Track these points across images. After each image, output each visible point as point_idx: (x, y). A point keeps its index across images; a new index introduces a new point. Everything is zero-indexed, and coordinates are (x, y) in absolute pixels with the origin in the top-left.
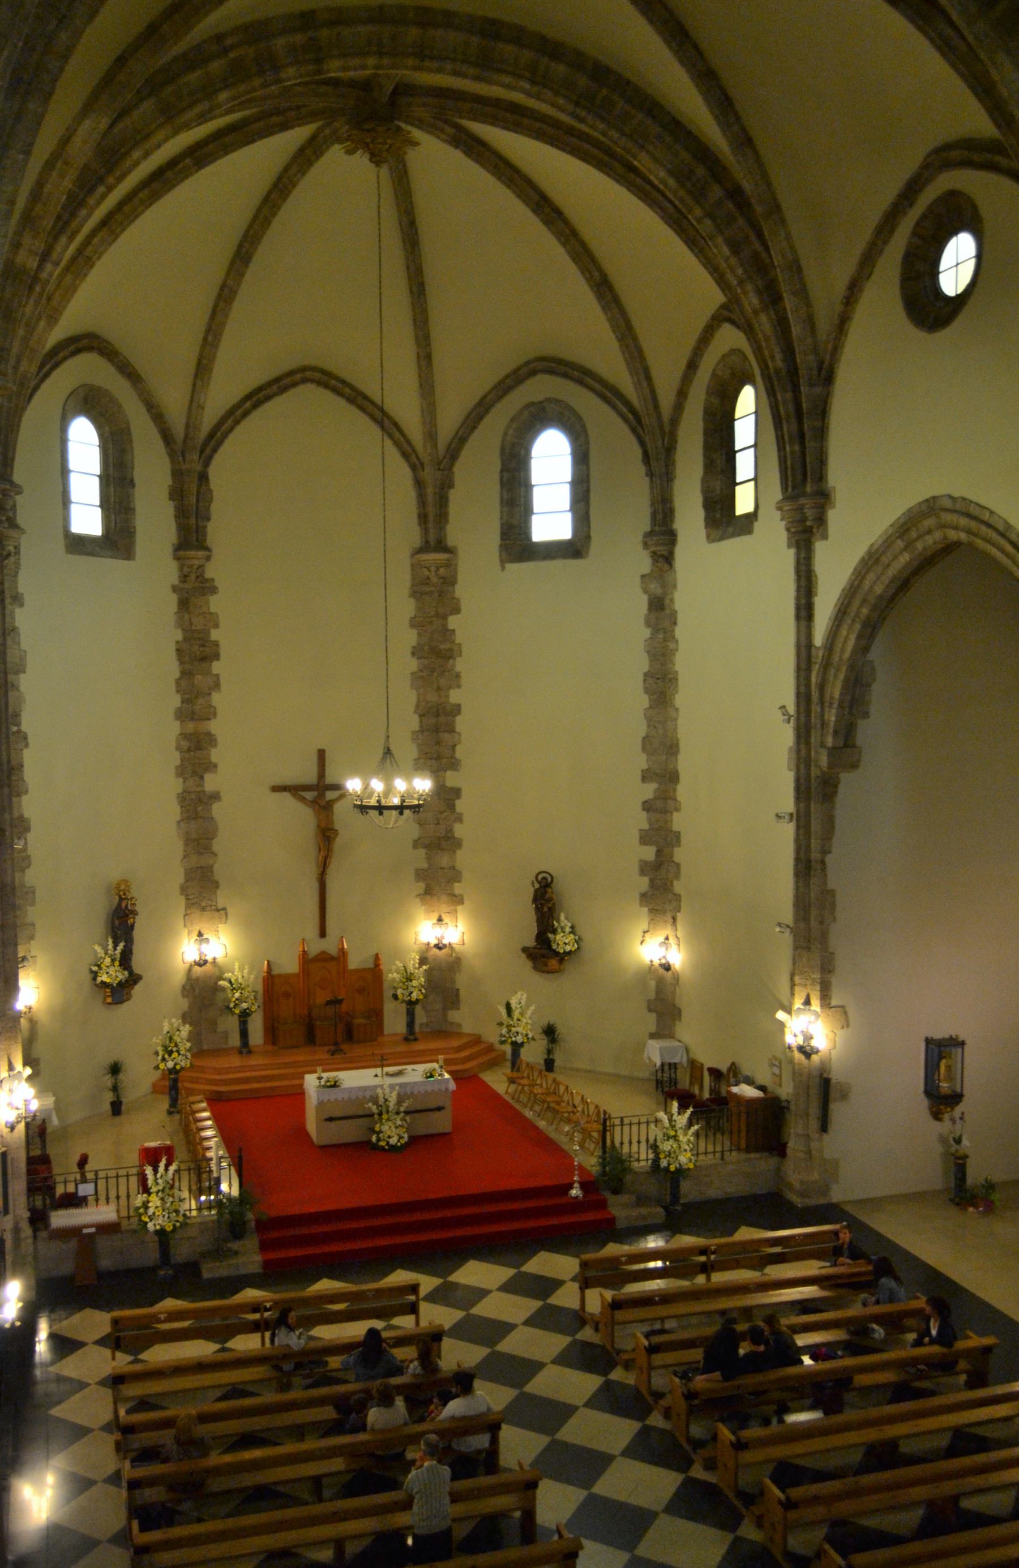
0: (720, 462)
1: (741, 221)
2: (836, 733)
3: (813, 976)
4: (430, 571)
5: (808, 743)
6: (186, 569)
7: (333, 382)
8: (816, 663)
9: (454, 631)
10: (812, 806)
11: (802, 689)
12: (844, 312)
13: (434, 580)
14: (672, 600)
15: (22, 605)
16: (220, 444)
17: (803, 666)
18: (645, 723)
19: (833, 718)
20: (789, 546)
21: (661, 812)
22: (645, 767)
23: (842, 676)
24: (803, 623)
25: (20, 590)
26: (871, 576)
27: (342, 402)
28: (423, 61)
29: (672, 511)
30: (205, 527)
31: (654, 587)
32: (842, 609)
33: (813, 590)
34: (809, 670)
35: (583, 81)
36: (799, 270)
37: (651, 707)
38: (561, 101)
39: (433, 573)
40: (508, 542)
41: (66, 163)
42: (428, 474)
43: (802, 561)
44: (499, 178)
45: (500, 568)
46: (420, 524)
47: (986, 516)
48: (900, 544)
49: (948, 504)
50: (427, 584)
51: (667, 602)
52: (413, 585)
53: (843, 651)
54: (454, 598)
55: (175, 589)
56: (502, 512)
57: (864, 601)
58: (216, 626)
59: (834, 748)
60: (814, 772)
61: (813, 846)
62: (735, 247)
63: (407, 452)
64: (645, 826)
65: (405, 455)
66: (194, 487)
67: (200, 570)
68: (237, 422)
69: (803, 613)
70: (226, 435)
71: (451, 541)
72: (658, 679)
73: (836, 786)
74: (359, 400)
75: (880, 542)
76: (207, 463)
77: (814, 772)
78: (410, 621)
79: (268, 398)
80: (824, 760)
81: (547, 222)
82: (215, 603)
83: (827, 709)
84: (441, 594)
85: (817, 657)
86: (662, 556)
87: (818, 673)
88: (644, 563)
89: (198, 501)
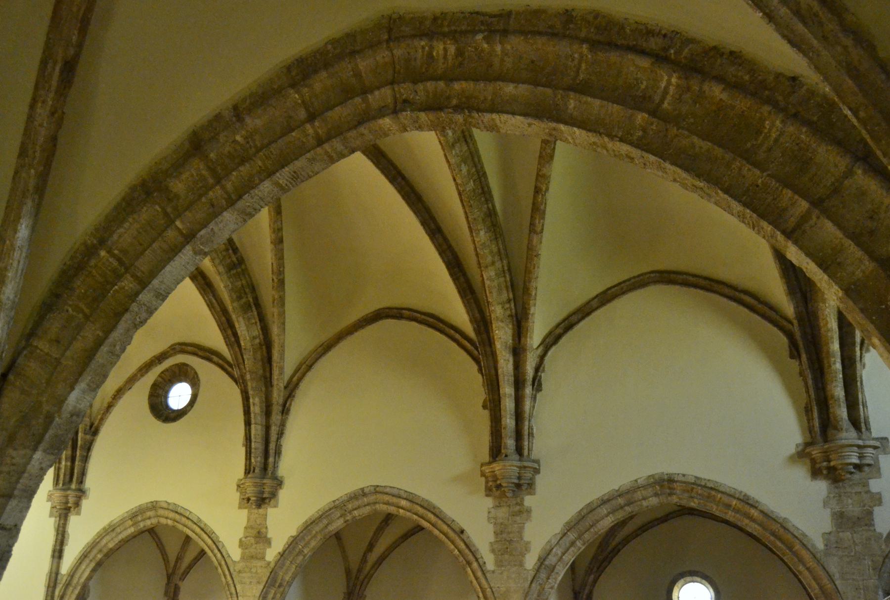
8: (60, 583)
12: (111, 402)
17: (52, 585)
20: (51, 515)
23: (77, 592)
24: (56, 560)
26: (108, 538)
32: (85, 554)
33: (65, 542)
34: (55, 587)
43: (61, 525)
47: (187, 514)
48: (130, 523)
49: (165, 505)
53: (80, 578)
57: (100, 551)
69: (57, 554)
75: (118, 520)
85: (62, 580)
87: (61, 590)
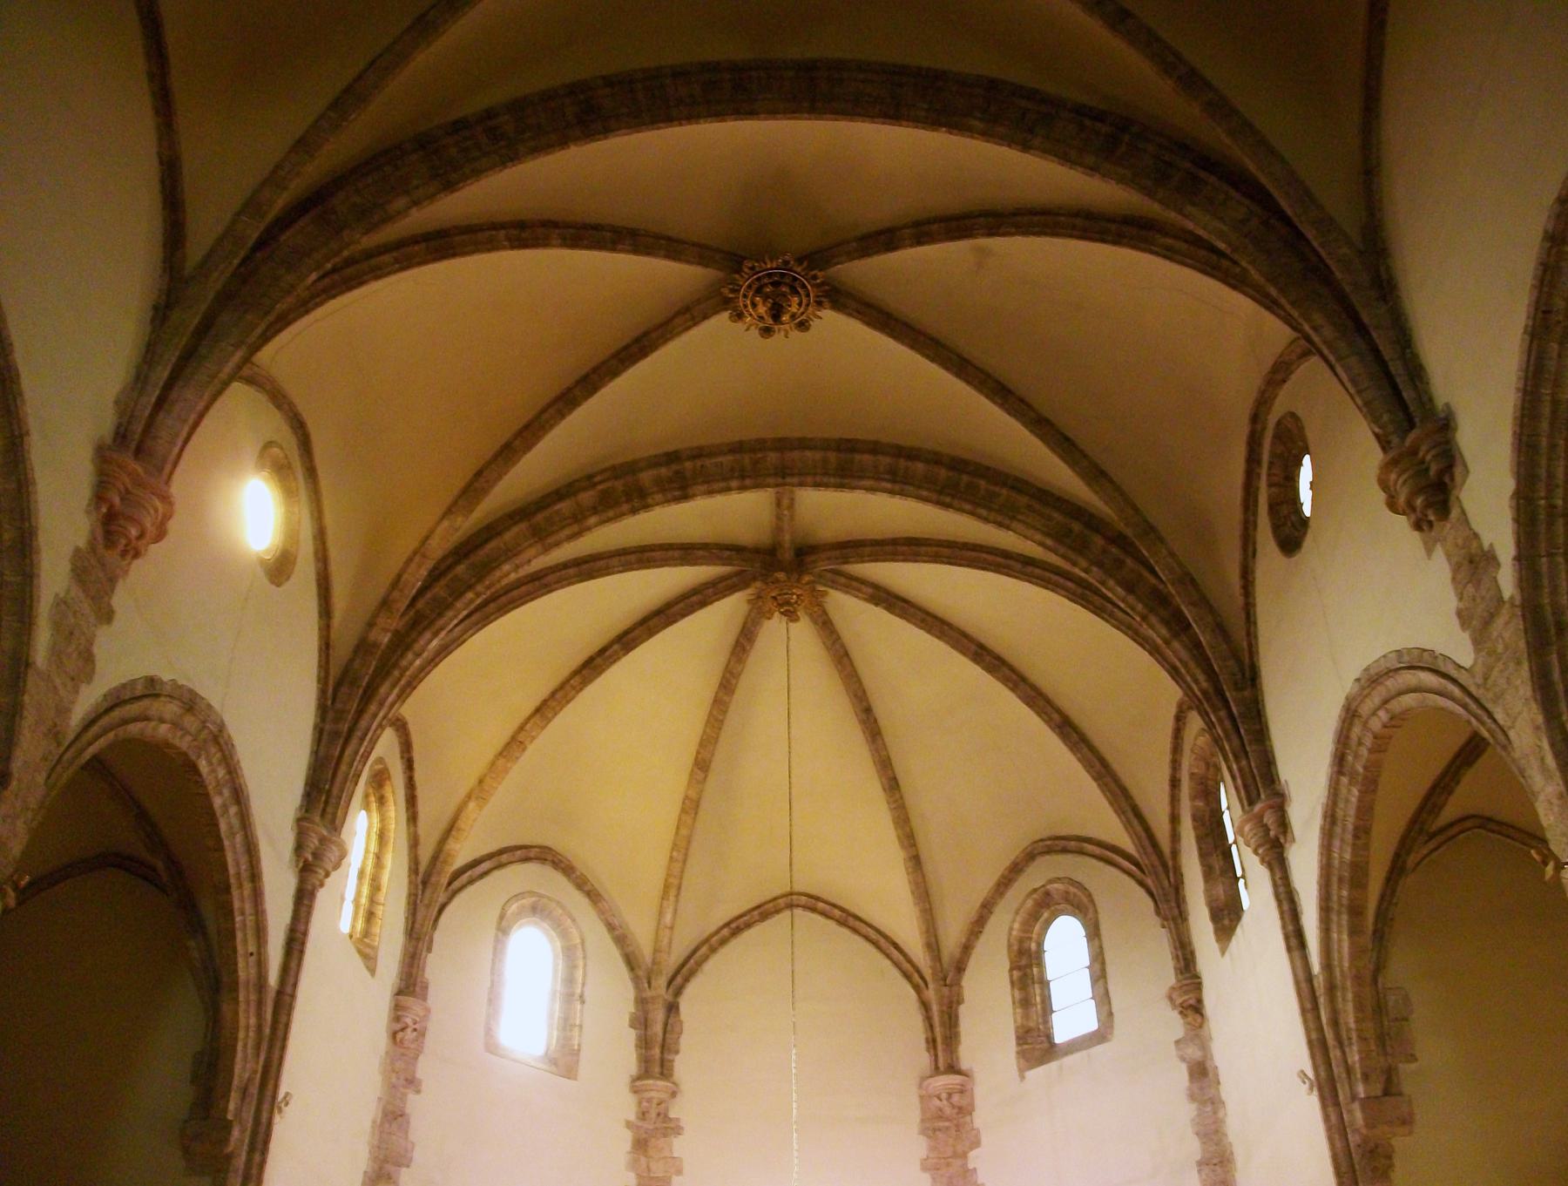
0: (1217, 862)
1: (1129, 562)
2: (1366, 1077)
4: (941, 1100)
5: (1337, 1104)
6: (645, 1104)
7: (821, 905)
9: (975, 1169)
11: (1314, 1036)
13: (948, 1111)
14: (1212, 1059)
15: (418, 1092)
16: (692, 973)
17: (1308, 1006)
19: (1357, 1058)
23: (1350, 996)
24: (1296, 954)
25: (420, 1074)
26: (1337, 843)
27: (831, 924)
28: (784, 478)
29: (1192, 953)
30: (673, 1061)
31: (1193, 1052)
34: (1316, 1008)
35: (943, 473)
38: (925, 493)
39: (945, 1102)
40: (1026, 1047)
41: (424, 556)
42: (931, 994)
43: (1279, 882)
44: (929, 632)
45: (1018, 1079)
46: (928, 1050)
50: (941, 1117)
51: (1208, 1064)
52: (923, 1121)
54: (973, 1129)
55: (629, 1125)
56: (1015, 1014)
57: (1340, 880)
58: (679, 1172)
59: (1368, 1098)
60: (1353, 1139)
62: (1130, 588)
63: (910, 972)
65: (907, 976)
66: (659, 1015)
67: (663, 1105)
68: (713, 950)
69: (1294, 942)
70: (699, 964)
71: (964, 1064)
72: (1215, 1165)
73: (1389, 1157)
74: (851, 921)
76: (678, 992)
77: (1353, 1139)
78: (922, 1164)
79: (748, 926)
80: (1359, 1115)
81: (990, 669)
82: (680, 1146)
83: (1347, 1050)
84: (958, 1127)
86: (1191, 1006)
88: (1174, 1025)
89: (665, 1032)
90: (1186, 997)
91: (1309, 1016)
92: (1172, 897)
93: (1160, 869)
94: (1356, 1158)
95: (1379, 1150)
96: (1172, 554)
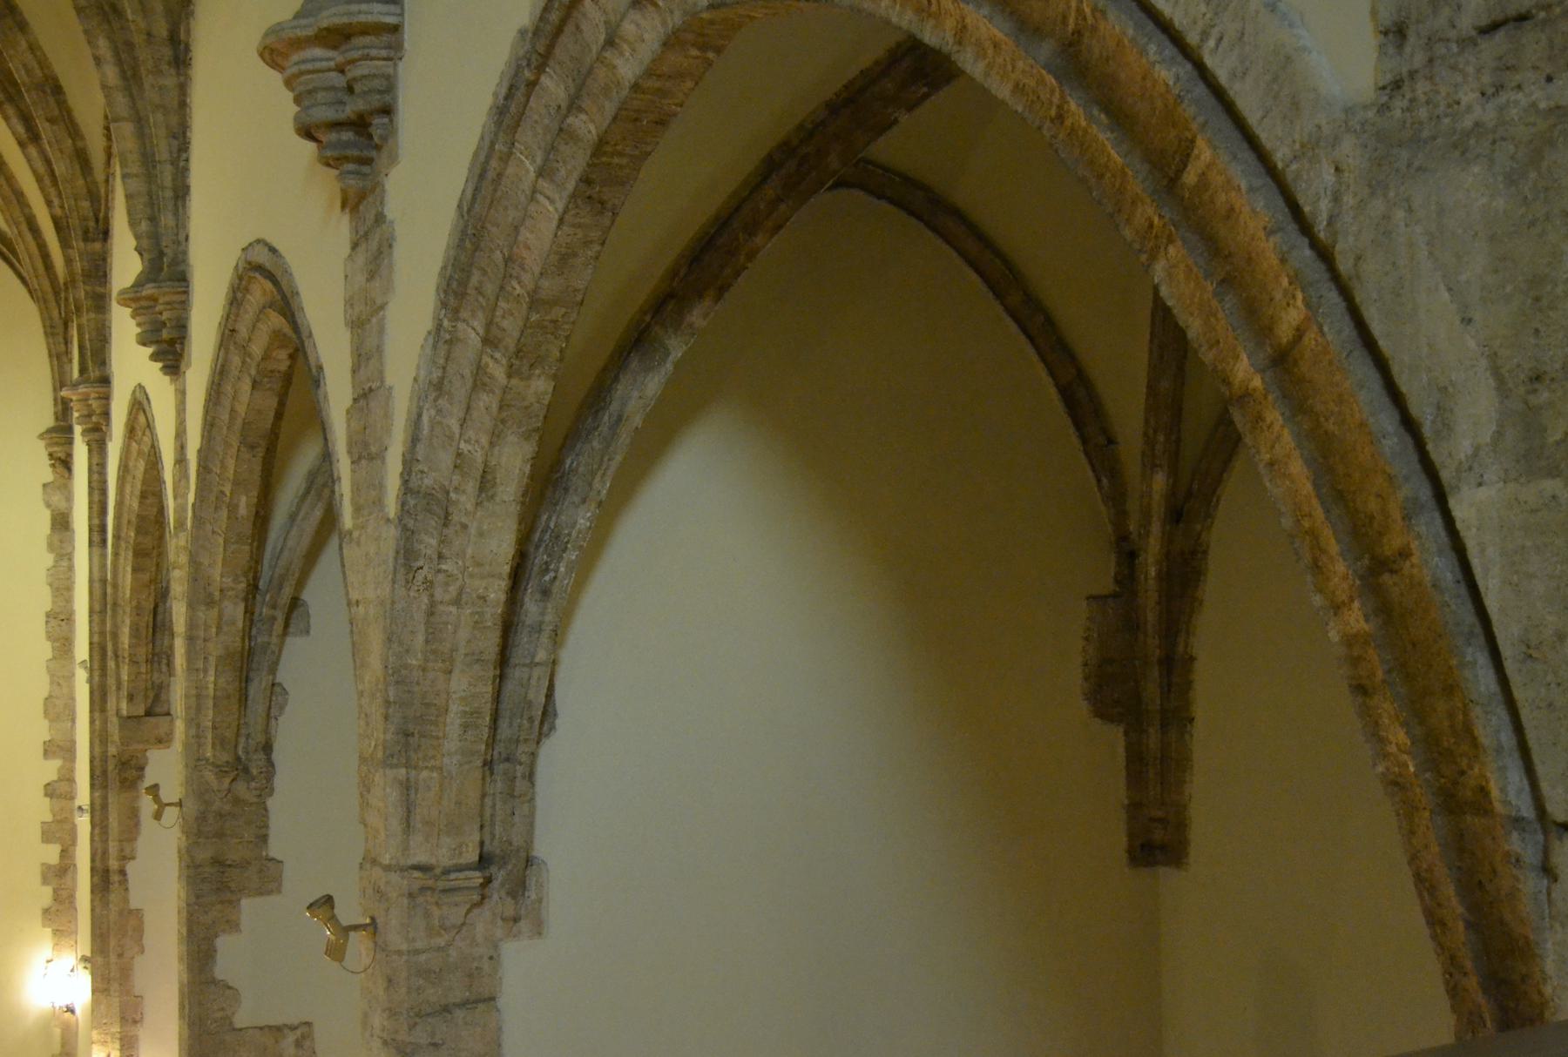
2: (131, 698)
3: (113, 1030)
5: (103, 710)
10: (110, 795)
11: (96, 639)
17: (97, 607)
18: (46, 679)
21: (65, 798)
22: (48, 738)
23: (128, 622)
24: (97, 551)
36: (58, 90)
37: (54, 658)
43: (95, 468)
59: (129, 717)
61: (111, 850)
64: (49, 818)
69: (96, 538)
73: (142, 769)
77: (112, 750)
83: (121, 665)
86: (60, 459)
90: (56, 449)
91: (96, 617)
92: (60, 329)
93: (50, 296)
94: (111, 767)
95: (133, 763)
96: (33, 48)
